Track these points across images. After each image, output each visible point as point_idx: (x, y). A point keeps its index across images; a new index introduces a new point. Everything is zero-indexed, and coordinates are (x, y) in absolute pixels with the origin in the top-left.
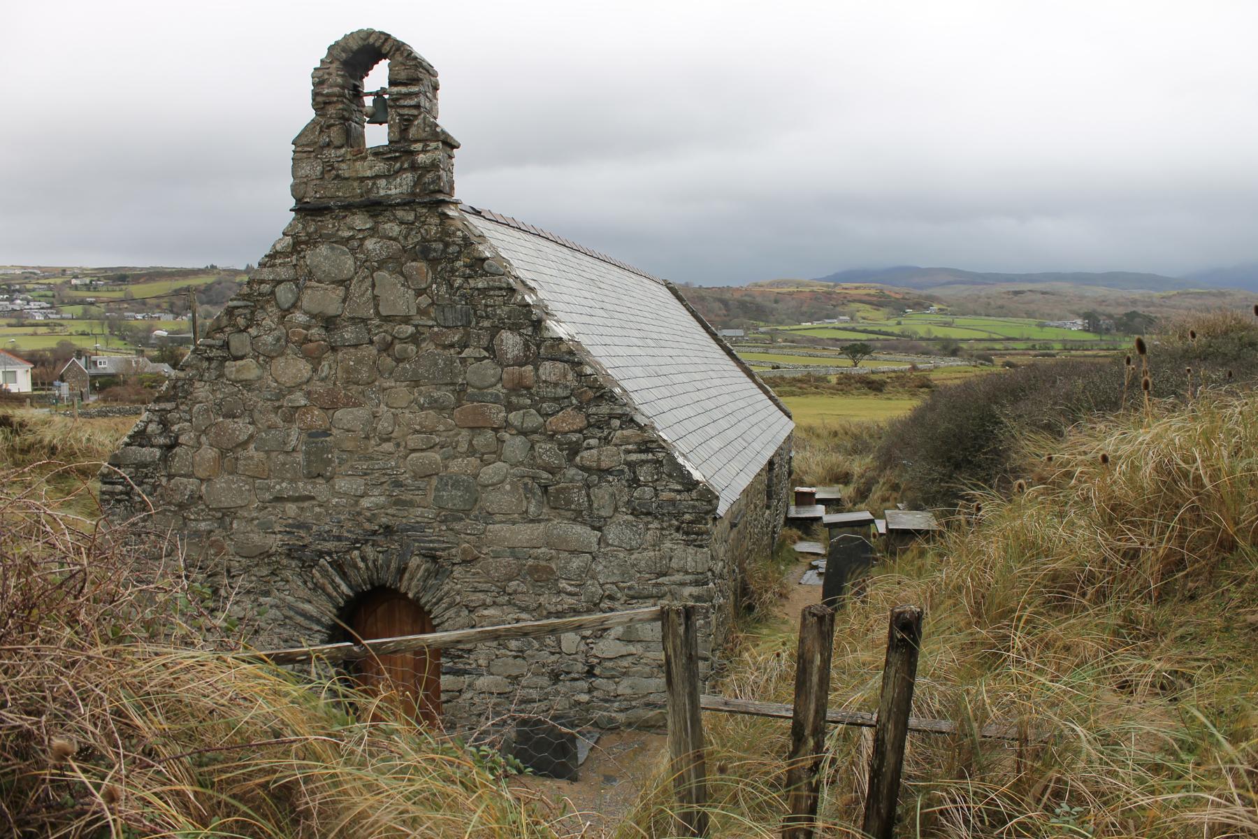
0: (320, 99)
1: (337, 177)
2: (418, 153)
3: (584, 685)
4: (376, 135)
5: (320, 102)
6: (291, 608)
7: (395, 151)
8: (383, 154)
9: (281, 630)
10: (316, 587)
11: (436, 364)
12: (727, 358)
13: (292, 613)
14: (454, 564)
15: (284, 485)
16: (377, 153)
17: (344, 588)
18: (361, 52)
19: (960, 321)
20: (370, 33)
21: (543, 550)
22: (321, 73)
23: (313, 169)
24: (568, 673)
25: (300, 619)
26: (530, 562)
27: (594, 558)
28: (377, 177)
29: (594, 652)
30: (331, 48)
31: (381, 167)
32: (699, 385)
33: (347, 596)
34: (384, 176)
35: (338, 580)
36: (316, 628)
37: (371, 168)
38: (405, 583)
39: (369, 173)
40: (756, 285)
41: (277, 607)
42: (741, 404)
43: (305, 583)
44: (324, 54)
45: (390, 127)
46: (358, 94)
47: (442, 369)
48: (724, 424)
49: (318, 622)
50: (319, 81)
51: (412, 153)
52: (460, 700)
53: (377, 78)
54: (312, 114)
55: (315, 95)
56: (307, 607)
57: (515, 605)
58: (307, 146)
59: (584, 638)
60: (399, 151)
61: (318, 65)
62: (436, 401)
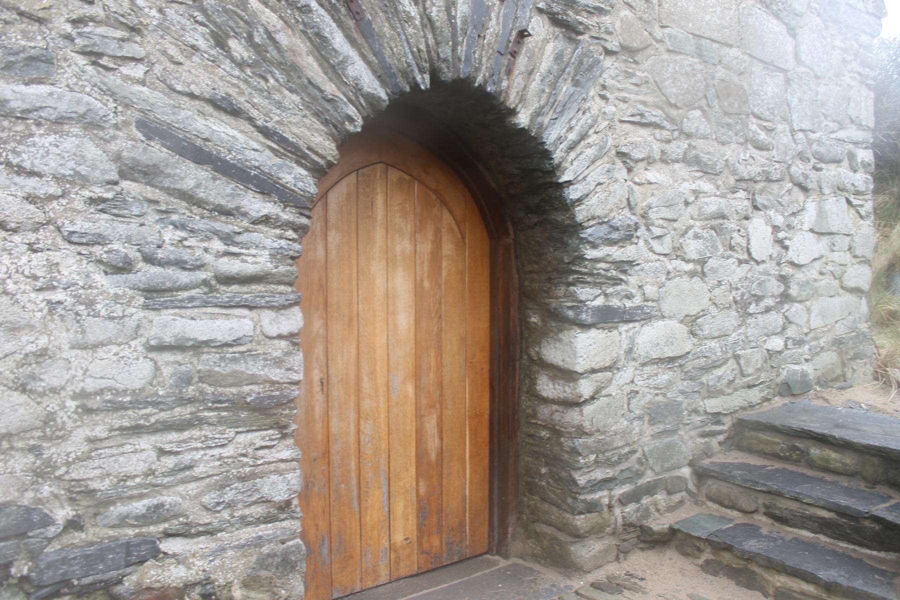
3: (775, 319)
6: (150, 129)
9: (103, 223)
10: (266, 58)
13: (158, 152)
14: (608, 53)
17: (360, 71)
21: (734, 52)
24: (758, 299)
25: (192, 176)
26: (721, 73)
27: (788, 81)
29: (791, 255)
33: (371, 99)
35: (338, 40)
36: (257, 205)
38: (518, 81)
41: (91, 124)
43: (220, 41)
49: (266, 186)
52: (612, 390)
56: (223, 132)
57: (697, 161)
59: (776, 229)
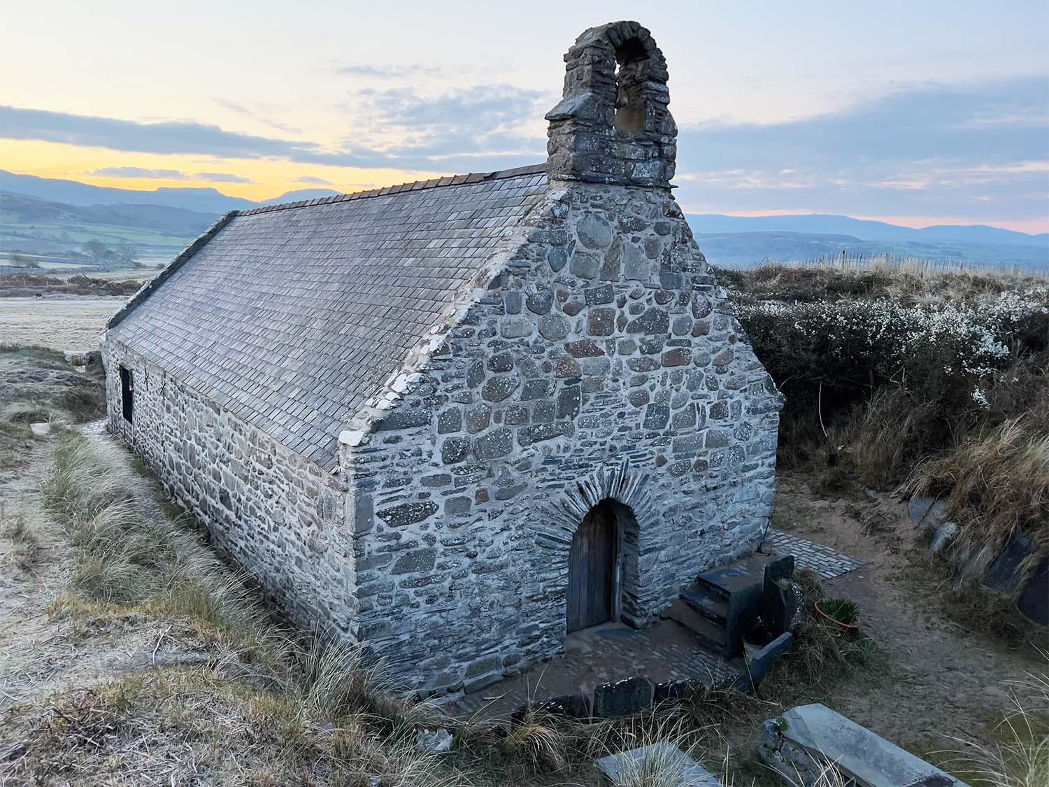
1: (610, 154)
11: (655, 319)
15: (541, 428)
28: (638, 160)
37: (635, 151)
39: (633, 157)
62: (653, 347)
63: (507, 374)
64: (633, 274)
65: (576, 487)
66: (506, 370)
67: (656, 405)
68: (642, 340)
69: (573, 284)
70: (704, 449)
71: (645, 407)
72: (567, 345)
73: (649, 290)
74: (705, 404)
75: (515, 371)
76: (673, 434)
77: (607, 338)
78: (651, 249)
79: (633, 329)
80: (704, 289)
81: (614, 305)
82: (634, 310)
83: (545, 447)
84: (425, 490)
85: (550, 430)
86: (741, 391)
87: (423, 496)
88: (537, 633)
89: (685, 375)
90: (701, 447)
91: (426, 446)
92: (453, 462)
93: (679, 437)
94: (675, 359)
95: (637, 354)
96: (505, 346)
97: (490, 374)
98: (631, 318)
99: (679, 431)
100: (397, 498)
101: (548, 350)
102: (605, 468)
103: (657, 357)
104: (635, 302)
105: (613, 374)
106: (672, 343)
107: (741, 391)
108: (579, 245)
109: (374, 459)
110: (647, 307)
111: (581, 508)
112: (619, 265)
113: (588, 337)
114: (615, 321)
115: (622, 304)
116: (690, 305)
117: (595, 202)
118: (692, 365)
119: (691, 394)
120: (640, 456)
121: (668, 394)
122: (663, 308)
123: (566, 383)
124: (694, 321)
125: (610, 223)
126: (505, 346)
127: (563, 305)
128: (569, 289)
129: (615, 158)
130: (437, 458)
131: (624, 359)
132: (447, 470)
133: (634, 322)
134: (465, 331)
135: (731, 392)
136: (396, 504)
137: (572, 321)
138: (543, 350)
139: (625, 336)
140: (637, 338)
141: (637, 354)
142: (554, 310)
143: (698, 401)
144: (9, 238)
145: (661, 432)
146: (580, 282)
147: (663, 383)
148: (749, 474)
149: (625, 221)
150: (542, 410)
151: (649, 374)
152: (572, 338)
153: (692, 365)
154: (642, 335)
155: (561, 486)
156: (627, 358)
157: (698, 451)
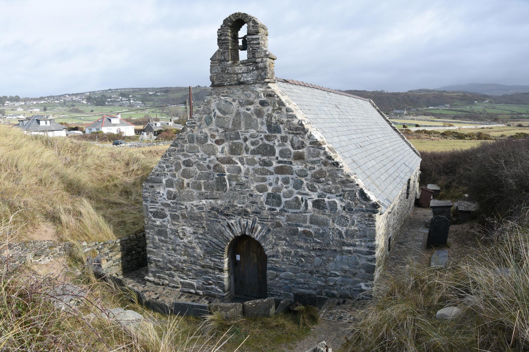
0: (220, 42)
1: (228, 72)
2: (259, 63)
4: (243, 55)
5: (221, 42)
7: (250, 62)
8: (245, 63)
11: (267, 149)
12: (394, 131)
15: (208, 193)
16: (243, 63)
18: (236, 22)
19: (498, 106)
20: (239, 14)
22: (221, 31)
23: (218, 69)
30: (224, 21)
31: (244, 68)
32: (379, 148)
34: (246, 73)
39: (240, 71)
40: (410, 91)
42: (397, 154)
44: (222, 23)
45: (248, 52)
46: (235, 38)
47: (269, 151)
48: (388, 166)
50: (221, 34)
51: (256, 63)
53: (243, 32)
54: (217, 48)
55: (219, 40)
58: (217, 60)
60: (252, 61)
61: (220, 28)
63: (191, 168)
64: (249, 126)
65: (226, 224)
66: (190, 166)
67: (272, 194)
68: (260, 159)
69: (218, 131)
70: (308, 224)
71: (266, 193)
72: (217, 158)
73: (260, 134)
74: (307, 199)
75: (195, 166)
76: (286, 211)
77: (239, 156)
78: (259, 113)
79: (254, 152)
80: (297, 134)
81: (241, 141)
82: (253, 144)
83: (210, 202)
84: (162, 207)
85: (213, 195)
86: (337, 196)
87: (162, 210)
88: (211, 282)
89: (291, 181)
90: (306, 223)
91: (162, 192)
92: (170, 199)
93: (290, 214)
94: (279, 171)
95: (257, 166)
96: (188, 156)
97: (183, 167)
98: (252, 148)
99: (290, 211)
100: (154, 208)
101: (208, 159)
102: (242, 220)
103: (271, 169)
104: (254, 140)
105: (245, 174)
106: (280, 162)
107: (337, 196)
108: (218, 113)
109: (147, 192)
110: (261, 142)
111: (231, 236)
112: (240, 122)
113: (229, 155)
114: (243, 148)
115: (246, 140)
116: (289, 142)
117: (223, 95)
118: (295, 176)
119: (296, 191)
120: (264, 218)
121: (279, 189)
122: (271, 143)
123: (218, 175)
124: (293, 151)
125: (233, 103)
126: (188, 156)
127: (214, 140)
128: (216, 134)
129: (231, 74)
130: (165, 196)
131: (251, 168)
132: (169, 202)
133: (254, 150)
134: (172, 150)
135: (328, 195)
136: (155, 210)
137: (219, 148)
138: (205, 159)
139: (250, 156)
140: (257, 158)
141: (257, 166)
142: (209, 142)
143: (303, 196)
144: (459, 113)
145: (278, 209)
146: (221, 130)
147: (277, 182)
148: (346, 248)
149: (241, 101)
150: (208, 186)
151: (267, 177)
152: (219, 155)
153: (295, 176)
154: (259, 156)
155: (220, 222)
156: (252, 167)
157: (304, 225)
